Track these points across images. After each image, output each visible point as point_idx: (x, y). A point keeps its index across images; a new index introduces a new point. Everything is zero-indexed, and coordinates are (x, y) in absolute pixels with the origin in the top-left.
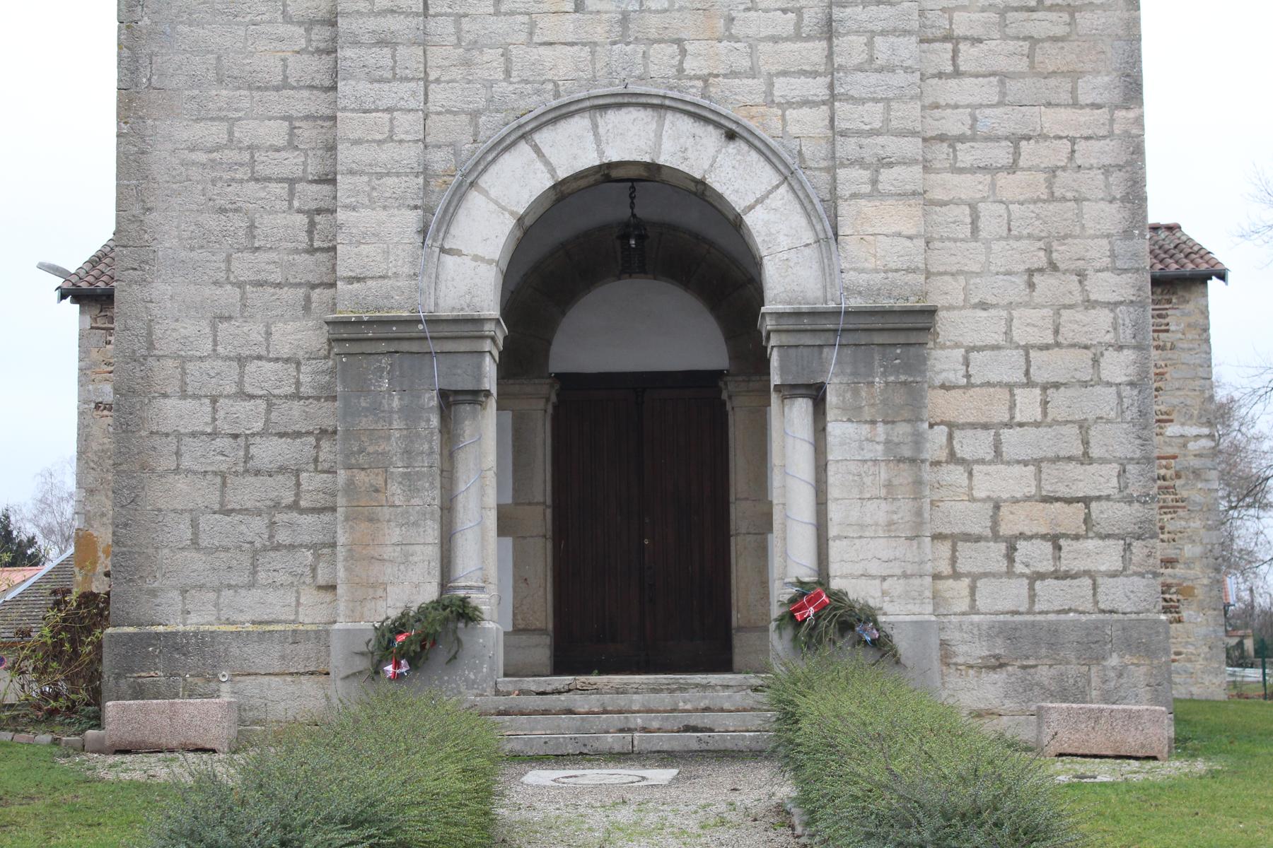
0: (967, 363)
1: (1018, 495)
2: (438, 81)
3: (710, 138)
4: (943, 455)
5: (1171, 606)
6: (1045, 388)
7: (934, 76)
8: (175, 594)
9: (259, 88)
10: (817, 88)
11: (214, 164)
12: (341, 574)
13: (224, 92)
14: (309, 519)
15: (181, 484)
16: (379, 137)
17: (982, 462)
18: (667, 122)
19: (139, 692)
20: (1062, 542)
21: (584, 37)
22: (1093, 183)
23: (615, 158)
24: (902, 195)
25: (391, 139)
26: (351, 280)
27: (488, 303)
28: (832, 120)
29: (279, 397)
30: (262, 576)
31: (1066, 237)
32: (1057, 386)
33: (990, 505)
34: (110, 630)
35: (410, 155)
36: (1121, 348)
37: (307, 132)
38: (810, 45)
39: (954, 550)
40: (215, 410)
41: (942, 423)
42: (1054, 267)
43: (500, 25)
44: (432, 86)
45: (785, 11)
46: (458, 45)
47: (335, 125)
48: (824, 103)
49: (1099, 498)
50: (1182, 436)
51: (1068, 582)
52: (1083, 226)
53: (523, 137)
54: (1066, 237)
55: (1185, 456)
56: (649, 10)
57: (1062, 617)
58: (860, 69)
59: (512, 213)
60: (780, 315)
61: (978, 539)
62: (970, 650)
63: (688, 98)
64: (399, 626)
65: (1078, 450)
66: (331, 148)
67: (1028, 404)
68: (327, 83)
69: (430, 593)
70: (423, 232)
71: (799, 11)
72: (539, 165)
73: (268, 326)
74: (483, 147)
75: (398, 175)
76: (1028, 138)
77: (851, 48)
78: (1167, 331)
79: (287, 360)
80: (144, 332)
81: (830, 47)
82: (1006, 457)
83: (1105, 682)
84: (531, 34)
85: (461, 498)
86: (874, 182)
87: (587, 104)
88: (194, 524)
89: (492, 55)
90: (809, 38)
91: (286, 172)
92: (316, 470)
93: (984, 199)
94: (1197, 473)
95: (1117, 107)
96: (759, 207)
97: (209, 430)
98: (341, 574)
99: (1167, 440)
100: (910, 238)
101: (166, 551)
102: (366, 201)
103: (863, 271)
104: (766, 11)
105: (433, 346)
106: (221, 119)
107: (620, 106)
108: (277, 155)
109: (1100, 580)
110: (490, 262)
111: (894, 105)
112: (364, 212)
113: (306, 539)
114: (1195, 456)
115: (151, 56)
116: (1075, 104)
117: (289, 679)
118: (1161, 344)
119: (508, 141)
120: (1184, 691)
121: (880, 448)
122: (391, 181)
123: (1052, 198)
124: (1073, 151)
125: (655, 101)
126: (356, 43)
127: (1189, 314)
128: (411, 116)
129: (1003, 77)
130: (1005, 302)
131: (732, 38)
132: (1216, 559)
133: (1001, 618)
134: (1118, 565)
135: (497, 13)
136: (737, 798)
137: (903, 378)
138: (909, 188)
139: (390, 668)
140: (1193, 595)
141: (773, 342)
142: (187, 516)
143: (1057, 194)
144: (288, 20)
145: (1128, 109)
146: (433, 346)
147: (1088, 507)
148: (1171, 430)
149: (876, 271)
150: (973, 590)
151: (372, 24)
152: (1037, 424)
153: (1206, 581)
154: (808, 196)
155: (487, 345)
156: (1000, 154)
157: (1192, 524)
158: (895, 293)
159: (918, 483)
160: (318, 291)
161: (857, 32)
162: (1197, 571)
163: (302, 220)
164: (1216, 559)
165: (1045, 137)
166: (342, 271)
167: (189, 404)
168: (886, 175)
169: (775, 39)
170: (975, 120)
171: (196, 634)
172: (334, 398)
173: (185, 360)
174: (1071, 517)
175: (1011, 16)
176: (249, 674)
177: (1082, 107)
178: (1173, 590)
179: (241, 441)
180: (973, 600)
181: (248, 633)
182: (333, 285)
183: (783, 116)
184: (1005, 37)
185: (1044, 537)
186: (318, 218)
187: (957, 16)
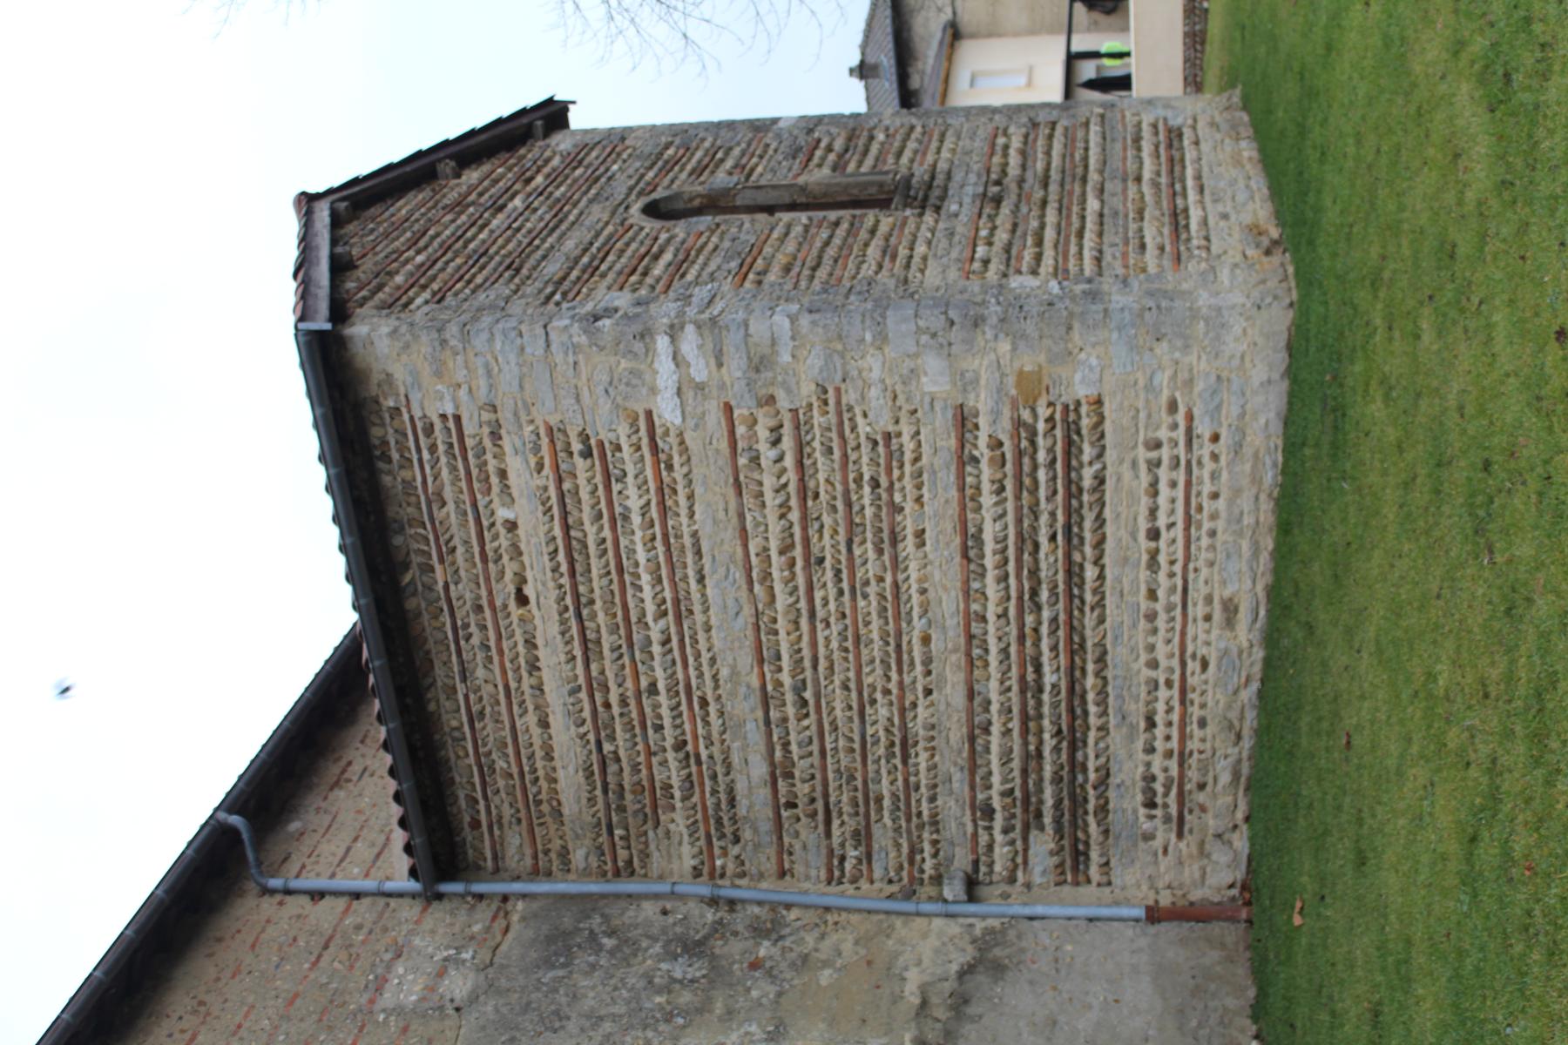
5: (1065, 420)
50: (679, 392)
55: (722, 386)
78: (458, 419)
94: (759, 364)
99: (691, 423)
114: (720, 365)
118: (486, 430)
120: (1260, 399)
127: (415, 374)
132: (952, 323)
140: (1039, 372)
148: (668, 411)
153: (1005, 346)
157: (876, 374)
162: (979, 364)
164: (952, 323)
178: (1026, 415)
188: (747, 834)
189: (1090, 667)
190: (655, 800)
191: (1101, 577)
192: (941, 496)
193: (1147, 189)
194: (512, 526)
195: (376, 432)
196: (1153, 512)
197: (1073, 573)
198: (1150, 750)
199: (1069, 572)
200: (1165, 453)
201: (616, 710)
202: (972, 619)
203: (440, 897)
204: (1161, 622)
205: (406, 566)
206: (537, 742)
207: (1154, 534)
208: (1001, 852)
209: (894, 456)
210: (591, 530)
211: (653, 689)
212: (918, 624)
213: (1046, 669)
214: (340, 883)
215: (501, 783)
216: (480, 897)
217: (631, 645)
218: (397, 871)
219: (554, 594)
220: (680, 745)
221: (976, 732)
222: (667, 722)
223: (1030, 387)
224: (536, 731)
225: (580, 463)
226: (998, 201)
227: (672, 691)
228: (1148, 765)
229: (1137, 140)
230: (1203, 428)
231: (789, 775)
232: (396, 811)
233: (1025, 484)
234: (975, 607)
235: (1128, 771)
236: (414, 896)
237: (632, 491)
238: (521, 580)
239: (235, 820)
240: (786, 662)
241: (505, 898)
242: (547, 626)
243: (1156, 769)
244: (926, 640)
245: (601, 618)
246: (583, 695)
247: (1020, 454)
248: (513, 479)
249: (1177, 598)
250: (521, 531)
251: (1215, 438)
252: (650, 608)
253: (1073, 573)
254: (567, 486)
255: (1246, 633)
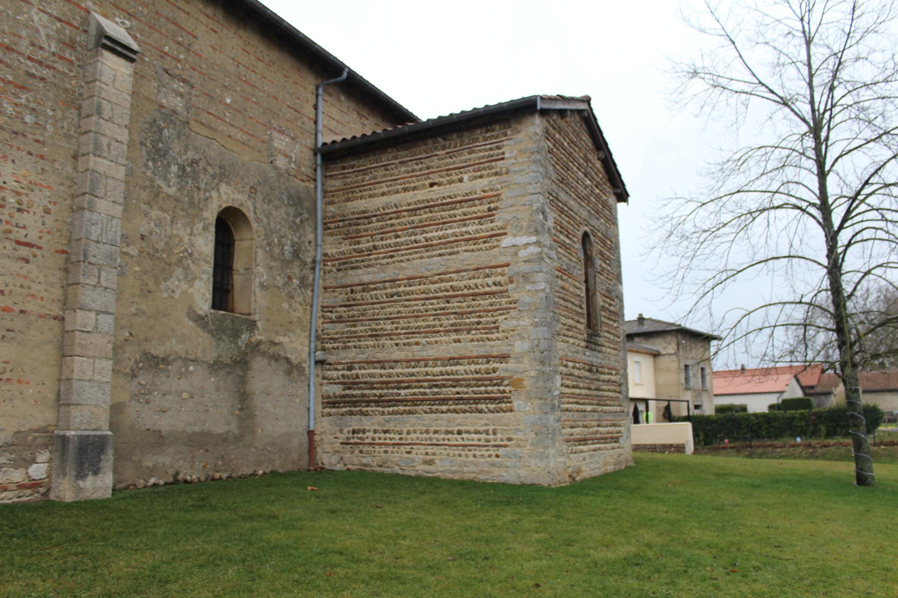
5: (504, 397)
50: (514, 246)
55: (516, 263)
78: (503, 159)
94: (525, 277)
99: (502, 250)
114: (525, 261)
118: (498, 170)
120: (513, 474)
127: (520, 142)
132: (542, 353)
140: (522, 387)
148: (506, 241)
153: (533, 373)
157: (522, 323)
162: (526, 364)
164: (542, 353)
178: (506, 382)
188: (341, 274)
189: (407, 408)
190: (353, 238)
191: (443, 412)
192: (474, 349)
193: (595, 429)
194: (461, 181)
195: (497, 127)
196: (468, 432)
197: (444, 401)
198: (375, 432)
199: (444, 399)
200: (491, 437)
201: (389, 222)
202: (426, 362)
203: (315, 154)
204: (425, 436)
205: (445, 140)
206: (376, 192)
207: (459, 432)
208: (334, 374)
209: (489, 330)
210: (460, 211)
211: (397, 237)
212: (423, 341)
213: (406, 391)
214: (320, 116)
215: (360, 178)
216: (315, 170)
217: (414, 228)
218: (325, 138)
219: (434, 197)
220: (375, 248)
221: (381, 363)
222: (384, 242)
223: (517, 383)
224: (380, 191)
225: (486, 207)
226: (590, 371)
227: (396, 244)
228: (369, 431)
229: (614, 425)
230: (501, 451)
231: (364, 290)
232: (349, 137)
233: (479, 382)
234: (430, 363)
235: (367, 423)
236: (316, 145)
237: (475, 227)
238: (440, 184)
239: (345, 75)
240: (408, 289)
241: (315, 180)
242: (422, 195)
243: (367, 434)
244: (417, 344)
245: (425, 216)
246: (395, 209)
247: (491, 380)
248: (479, 181)
249: (434, 442)
250: (459, 184)
251: (497, 456)
252: (429, 235)
253: (444, 401)
254: (477, 202)
255: (421, 469)
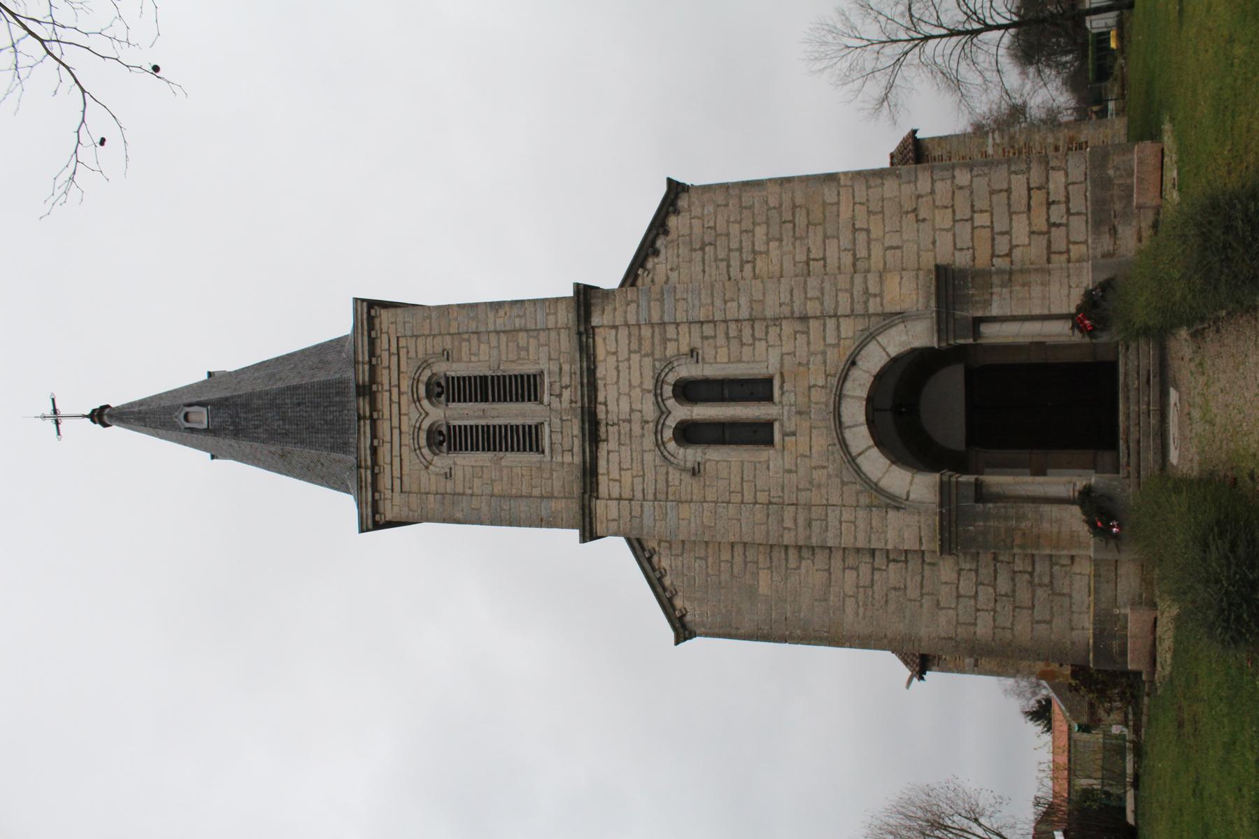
0: (961, 249)
1: (1027, 222)
2: (827, 500)
3: (855, 373)
4: (1007, 260)
6: (973, 211)
7: (825, 270)
8: (1074, 633)
9: (830, 583)
10: (831, 323)
11: (865, 605)
12: (1065, 552)
13: (831, 598)
14: (1038, 568)
15: (1018, 627)
16: (853, 528)
17: (1010, 241)
18: (848, 393)
19: (1124, 653)
20: (1051, 200)
21: (808, 431)
22: (875, 193)
23: (864, 418)
24: (881, 283)
25: (854, 523)
26: (921, 543)
27: (932, 479)
28: (846, 316)
29: (977, 580)
30: (1066, 591)
31: (900, 204)
32: (972, 206)
33: (1032, 236)
34: (1091, 665)
35: (861, 514)
36: (954, 177)
37: (850, 561)
38: (811, 327)
39: (1055, 253)
40: (983, 610)
41: (991, 260)
42: (915, 210)
43: (802, 471)
44: (830, 502)
45: (795, 339)
46: (811, 490)
47: (848, 549)
48: (838, 320)
49: (1028, 183)
51: (1071, 196)
52: (895, 197)
53: (854, 461)
54: (900, 204)
55: (1003, 144)
56: (795, 401)
57: (1089, 198)
58: (822, 304)
59: (890, 466)
60: (939, 340)
61: (1049, 241)
62: (1106, 243)
63: (836, 384)
64: (1092, 524)
65: (1005, 195)
66: (858, 550)
67: (982, 219)
68: (828, 551)
69: (1076, 510)
70: (898, 508)
71: (796, 332)
72: (867, 453)
73: (943, 583)
74: (858, 479)
75: (871, 520)
76: (854, 224)
77: (812, 308)
79: (959, 575)
80: (944, 641)
81: (811, 317)
82: (1008, 229)
83: (1122, 176)
84: (806, 456)
85: (1028, 493)
86: (875, 296)
87: (838, 431)
88: (1038, 622)
89: (816, 474)
90: (808, 328)
91: (869, 572)
92: (1014, 562)
93: (883, 244)
94: (1012, 138)
95: (839, 184)
96: (887, 350)
97: (992, 613)
98: (1065, 552)
100: (901, 278)
101: (1052, 636)
102: (883, 535)
103: (918, 300)
104: (795, 347)
105: (953, 506)
106: (844, 601)
107: (840, 416)
108: (861, 576)
109: (1070, 181)
110: (913, 477)
111: (839, 287)
112: (889, 536)
113: (1047, 569)
115: (814, 631)
116: (838, 203)
117: (1119, 580)
119: (856, 468)
121: (1004, 290)
122: (873, 522)
123: (882, 212)
124: (860, 203)
125: (837, 399)
126: (810, 537)
128: (844, 513)
129: (825, 237)
130: (932, 233)
131: (808, 363)
133: (1090, 228)
134: (1062, 173)
135: (796, 472)
136: (1187, 358)
137: (970, 280)
138: (878, 279)
139: (1115, 529)
141: (952, 342)
142: (1035, 626)
143: (880, 209)
144: (798, 568)
145: (840, 179)
146: (953, 506)
147: (1033, 189)
148: (990, 151)
149: (918, 293)
150: (1075, 243)
151: (801, 529)
152: (992, 215)
153: (1066, 131)
154: (882, 327)
155: (953, 479)
156: (861, 237)
158: (928, 284)
159: (1022, 271)
160: (926, 559)
161: (805, 305)
162: (1061, 135)
163: (892, 565)
165: (853, 216)
166: (916, 547)
167: (979, 622)
168: (872, 290)
169: (809, 343)
170: (845, 250)
171: (1094, 624)
172: (978, 553)
173: (958, 623)
174: (1038, 197)
175: (797, 235)
176: (1116, 599)
177: (839, 200)
179: (998, 598)
180: (1080, 243)
181: (1095, 598)
182: (923, 552)
183: (844, 339)
184: (807, 237)
185: (1048, 209)
186: (891, 558)
187: (797, 259)
